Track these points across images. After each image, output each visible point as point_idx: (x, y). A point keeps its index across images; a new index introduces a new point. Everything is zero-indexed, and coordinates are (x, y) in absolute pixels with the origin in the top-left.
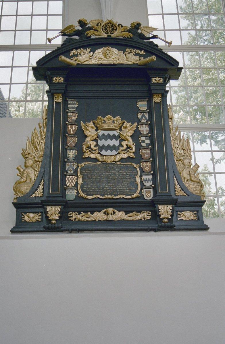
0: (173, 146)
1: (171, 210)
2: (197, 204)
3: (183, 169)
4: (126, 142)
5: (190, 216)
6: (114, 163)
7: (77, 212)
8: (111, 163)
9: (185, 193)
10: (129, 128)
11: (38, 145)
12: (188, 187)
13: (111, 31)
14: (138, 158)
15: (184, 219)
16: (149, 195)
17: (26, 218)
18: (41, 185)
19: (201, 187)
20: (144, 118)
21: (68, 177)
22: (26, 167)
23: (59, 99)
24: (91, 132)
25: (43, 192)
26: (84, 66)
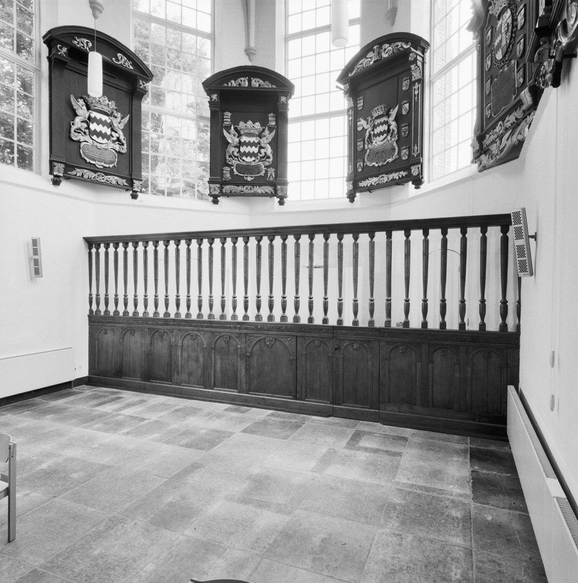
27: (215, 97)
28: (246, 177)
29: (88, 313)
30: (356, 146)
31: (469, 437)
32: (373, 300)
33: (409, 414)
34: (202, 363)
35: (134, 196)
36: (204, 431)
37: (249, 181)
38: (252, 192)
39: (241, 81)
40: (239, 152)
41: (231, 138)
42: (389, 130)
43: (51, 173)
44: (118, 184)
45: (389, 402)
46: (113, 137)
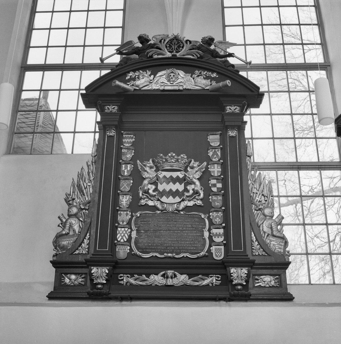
0: (251, 191)
1: (246, 274)
2: (280, 265)
3: (263, 221)
4: (193, 186)
5: (270, 281)
6: (177, 212)
7: (129, 274)
8: (173, 212)
9: (265, 252)
10: (196, 169)
11: (85, 189)
12: (268, 243)
13: (177, 49)
14: (206, 207)
15: (262, 285)
16: (218, 253)
17: (67, 281)
18: (87, 239)
19: (286, 244)
20: (215, 156)
21: (119, 229)
22: (70, 216)
23: (113, 133)
24: (149, 173)
25: (88, 248)
26: (142, 93)
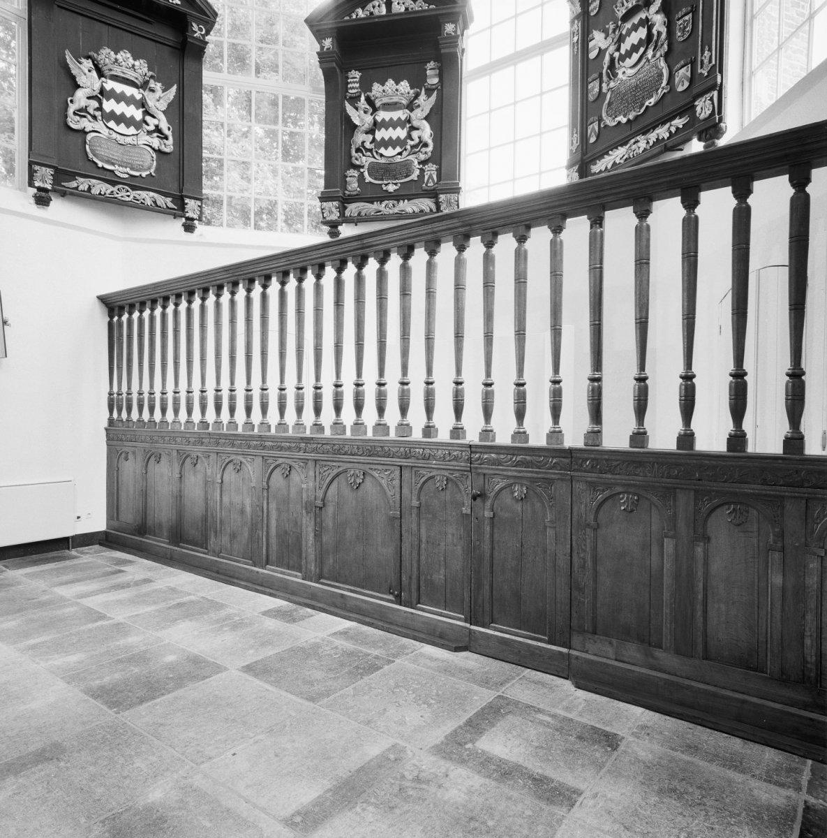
4: (156, 122)
27: (328, 43)
28: (386, 185)
29: (106, 424)
30: (585, 91)
31: (810, 762)
32: (558, 382)
33: (644, 670)
34: (249, 517)
35: (189, 228)
36: (171, 658)
37: (390, 193)
38: (396, 210)
39: (374, 7)
40: (374, 140)
41: (360, 117)
42: (650, 35)
43: (31, 184)
44: (157, 206)
45: (595, 633)
46: (148, 125)
